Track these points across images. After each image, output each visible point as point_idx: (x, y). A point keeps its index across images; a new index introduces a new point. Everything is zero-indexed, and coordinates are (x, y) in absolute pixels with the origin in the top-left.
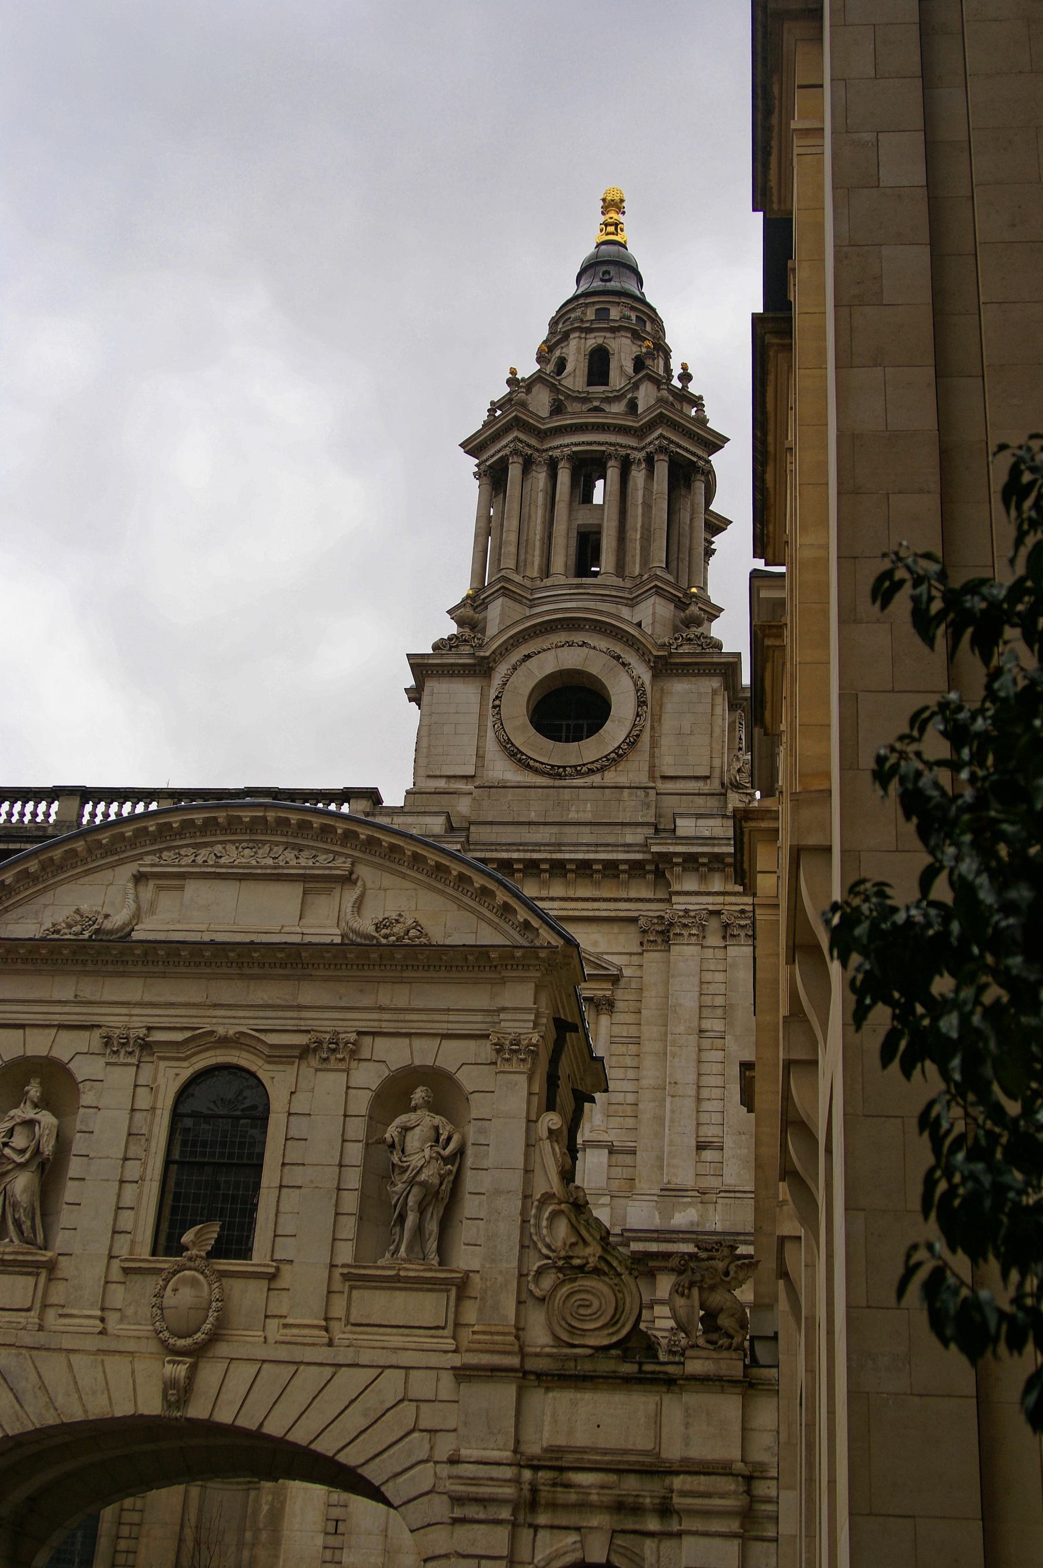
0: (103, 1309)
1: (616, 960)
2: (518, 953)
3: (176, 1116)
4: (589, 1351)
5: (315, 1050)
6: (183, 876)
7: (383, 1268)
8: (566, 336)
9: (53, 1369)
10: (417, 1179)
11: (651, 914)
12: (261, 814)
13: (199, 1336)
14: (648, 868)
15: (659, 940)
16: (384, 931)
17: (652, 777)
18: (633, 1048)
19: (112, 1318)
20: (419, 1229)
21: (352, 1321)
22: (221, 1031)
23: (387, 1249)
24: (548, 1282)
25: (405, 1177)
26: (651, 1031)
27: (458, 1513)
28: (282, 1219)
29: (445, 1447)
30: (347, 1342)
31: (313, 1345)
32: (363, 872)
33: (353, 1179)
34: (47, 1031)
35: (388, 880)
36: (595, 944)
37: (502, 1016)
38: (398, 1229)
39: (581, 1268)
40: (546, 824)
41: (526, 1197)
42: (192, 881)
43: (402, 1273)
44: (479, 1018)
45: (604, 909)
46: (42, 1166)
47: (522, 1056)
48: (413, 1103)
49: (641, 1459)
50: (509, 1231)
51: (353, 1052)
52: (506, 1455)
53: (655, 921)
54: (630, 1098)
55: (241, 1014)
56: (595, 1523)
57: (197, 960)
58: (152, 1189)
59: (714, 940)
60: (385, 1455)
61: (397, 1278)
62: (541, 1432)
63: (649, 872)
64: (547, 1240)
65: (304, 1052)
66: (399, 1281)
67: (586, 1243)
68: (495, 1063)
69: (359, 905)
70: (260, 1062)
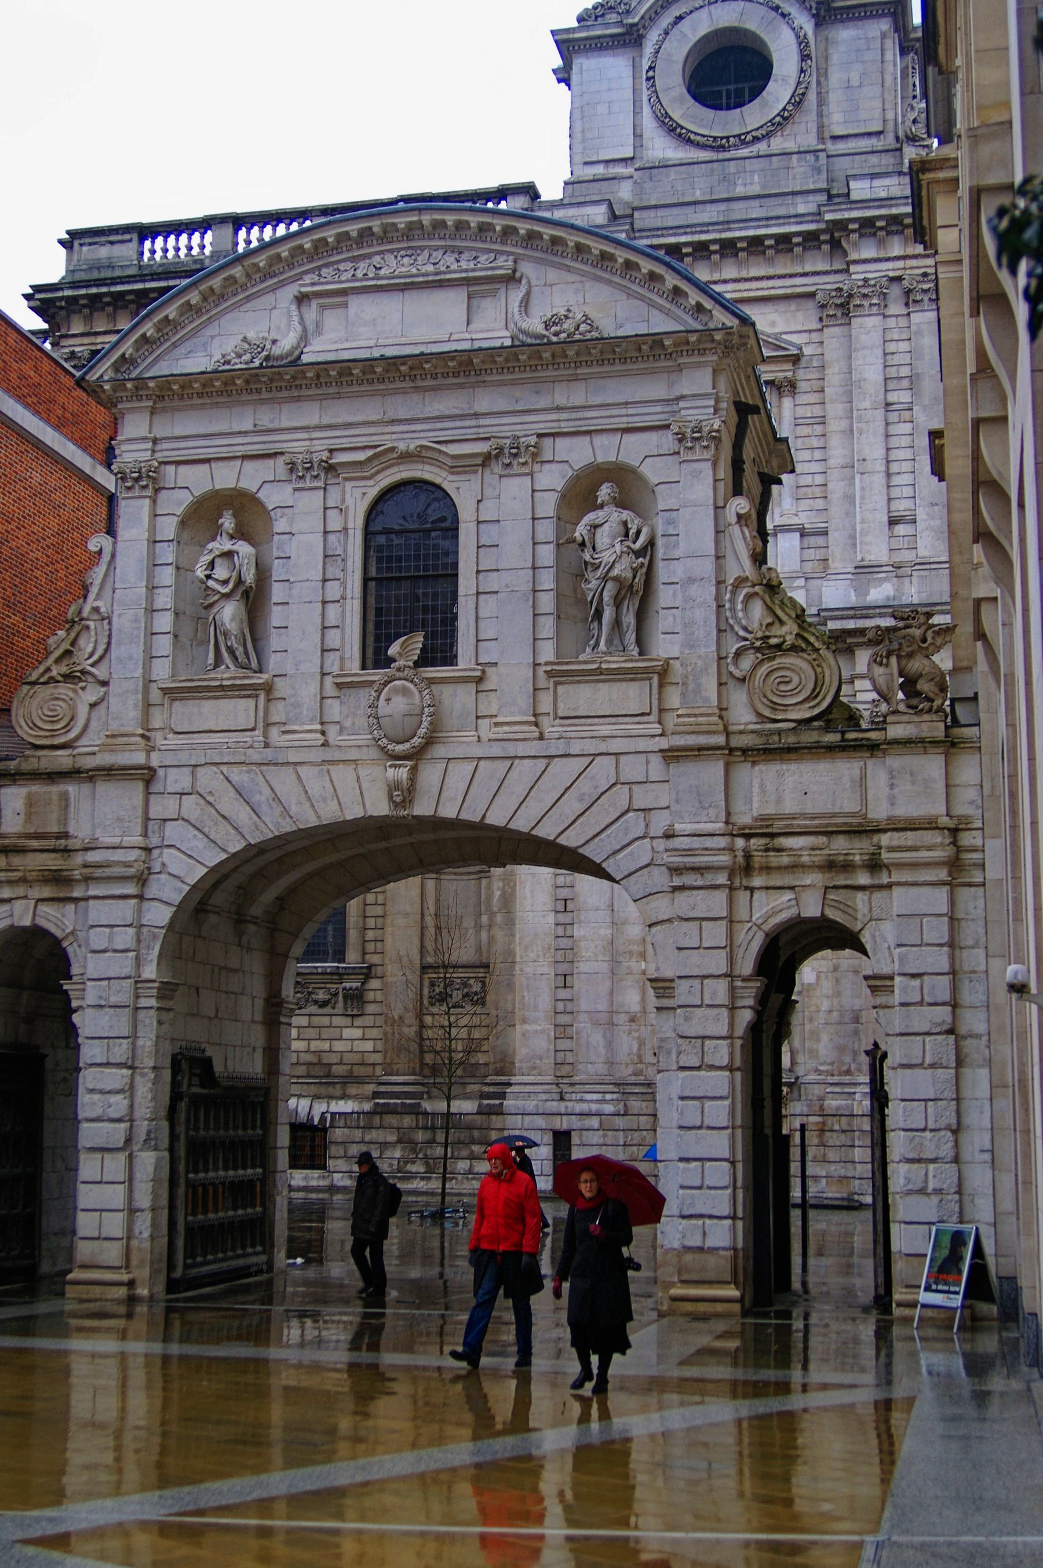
0: (322, 723)
1: (795, 339)
2: (693, 338)
3: (368, 534)
4: (792, 725)
5: (497, 456)
6: (344, 292)
7: (585, 662)
9: (284, 782)
10: (611, 574)
11: (829, 287)
12: (415, 219)
13: (416, 741)
14: (822, 238)
15: (839, 314)
16: (554, 329)
17: (821, 139)
18: (818, 429)
19: (332, 731)
20: (617, 623)
21: (560, 714)
22: (402, 446)
23: (587, 643)
24: (747, 662)
25: (599, 573)
26: (835, 410)
27: (677, 882)
28: (482, 624)
29: (660, 823)
30: (557, 735)
31: (525, 740)
32: (527, 269)
33: (547, 580)
34: (232, 463)
35: (552, 275)
36: (773, 324)
37: (682, 404)
38: (596, 624)
39: (779, 647)
40: (713, 202)
41: (719, 583)
42: (355, 297)
43: (604, 666)
44: (658, 409)
45: (779, 287)
46: (246, 594)
47: (705, 443)
48: (599, 501)
49: (849, 820)
50: (704, 616)
51: (534, 455)
52: (719, 826)
53: (834, 294)
54: (819, 479)
55: (419, 427)
56: (808, 882)
57: (370, 377)
58: (354, 606)
59: (896, 308)
60: (603, 835)
61: (600, 671)
62: (751, 802)
63: (825, 242)
64: (744, 622)
65: (487, 459)
66: (601, 674)
67: (782, 623)
68: (678, 453)
69: (525, 304)
70: (444, 474)
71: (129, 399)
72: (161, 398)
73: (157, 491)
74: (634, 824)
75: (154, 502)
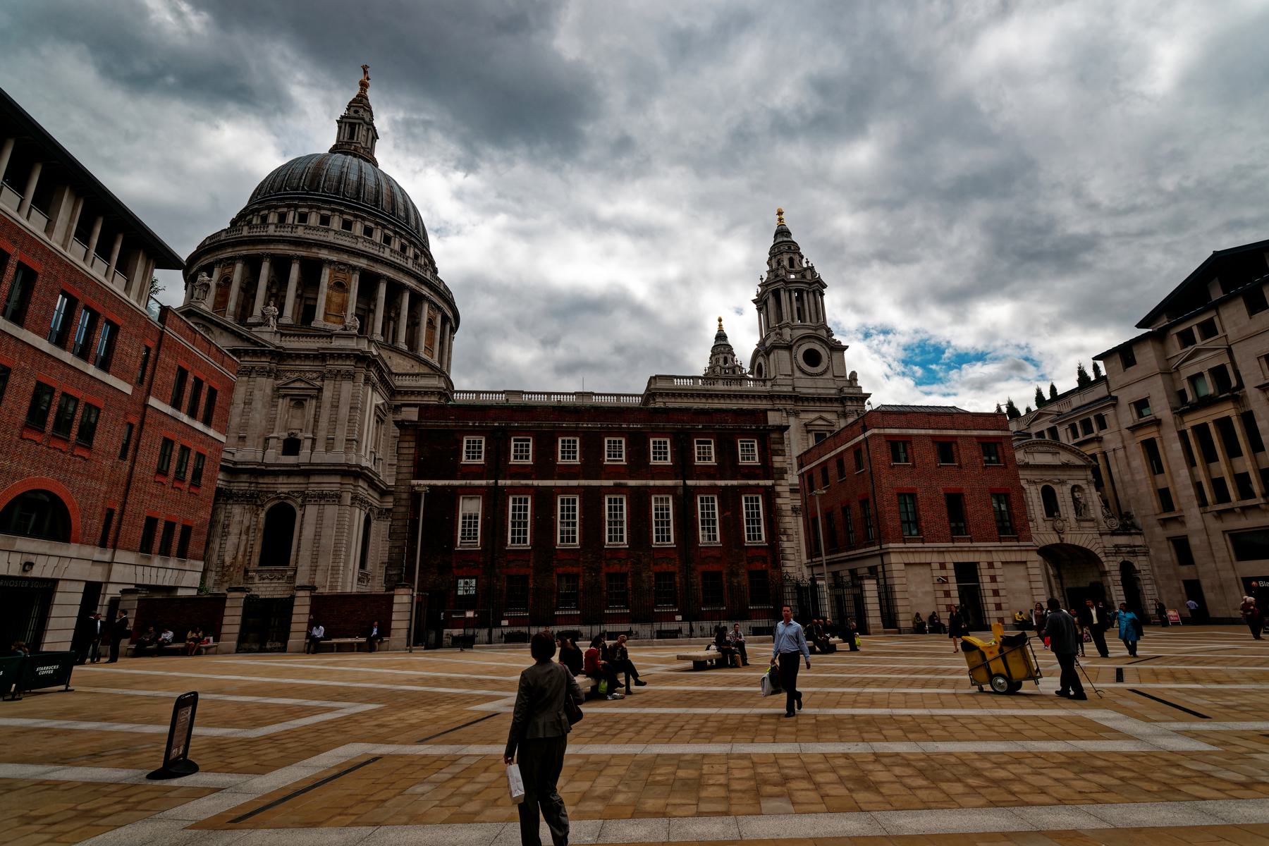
8: (782, 253)
9: (1042, 536)
29: (1101, 545)
45: (829, 409)
74: (1097, 545)
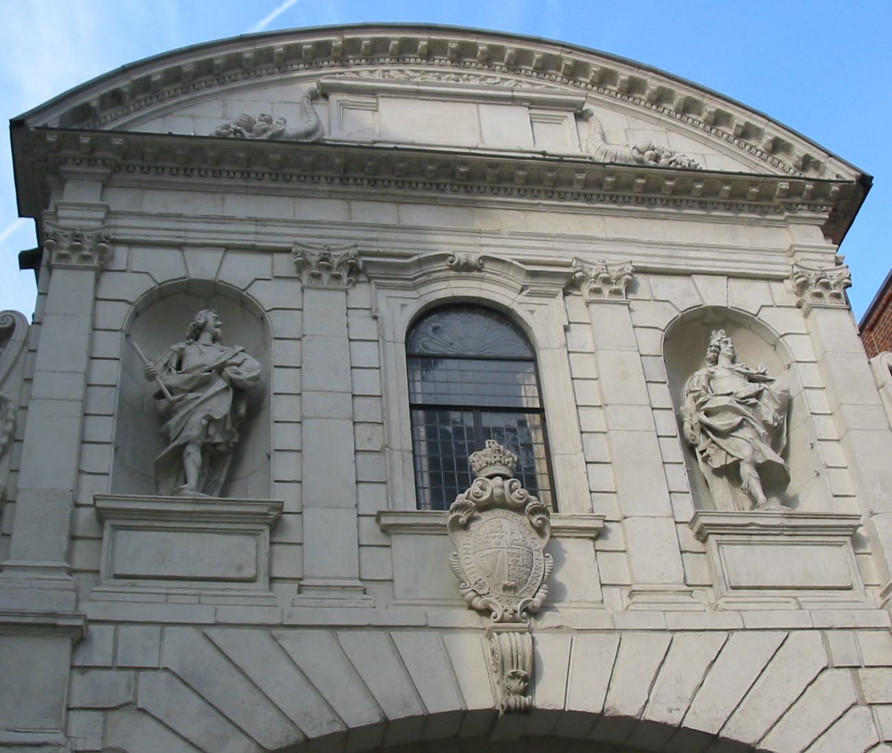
22: (461, 257)
70: (513, 295)
71: (78, 161)
72: (117, 168)
73: (101, 271)
75: (97, 281)
